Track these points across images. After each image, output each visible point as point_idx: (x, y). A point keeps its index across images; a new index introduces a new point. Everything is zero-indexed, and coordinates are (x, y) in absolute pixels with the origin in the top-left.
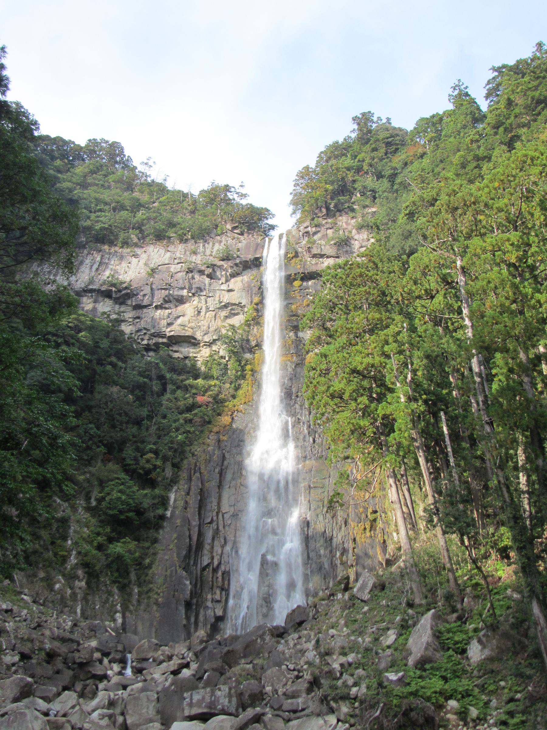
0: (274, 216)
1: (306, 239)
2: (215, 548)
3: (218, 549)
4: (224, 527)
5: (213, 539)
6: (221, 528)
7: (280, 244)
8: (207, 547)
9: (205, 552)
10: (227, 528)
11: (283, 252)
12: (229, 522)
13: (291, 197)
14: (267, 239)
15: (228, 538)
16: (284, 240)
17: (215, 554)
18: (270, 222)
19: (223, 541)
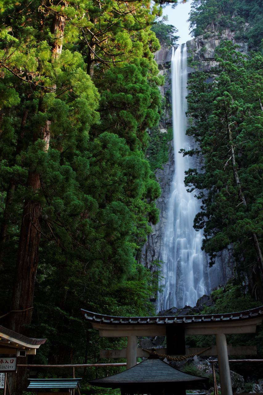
0: (177, 31)
1: (200, 48)
2: (148, 258)
3: (149, 257)
4: (153, 244)
5: (146, 252)
6: (151, 244)
7: (182, 52)
8: (143, 257)
9: (142, 260)
10: (155, 245)
11: (185, 57)
12: (156, 241)
13: (189, 16)
14: (173, 48)
15: (156, 251)
16: (185, 49)
17: (148, 261)
18: (175, 34)
19: (152, 252)
